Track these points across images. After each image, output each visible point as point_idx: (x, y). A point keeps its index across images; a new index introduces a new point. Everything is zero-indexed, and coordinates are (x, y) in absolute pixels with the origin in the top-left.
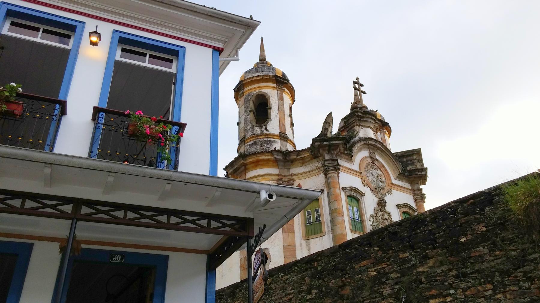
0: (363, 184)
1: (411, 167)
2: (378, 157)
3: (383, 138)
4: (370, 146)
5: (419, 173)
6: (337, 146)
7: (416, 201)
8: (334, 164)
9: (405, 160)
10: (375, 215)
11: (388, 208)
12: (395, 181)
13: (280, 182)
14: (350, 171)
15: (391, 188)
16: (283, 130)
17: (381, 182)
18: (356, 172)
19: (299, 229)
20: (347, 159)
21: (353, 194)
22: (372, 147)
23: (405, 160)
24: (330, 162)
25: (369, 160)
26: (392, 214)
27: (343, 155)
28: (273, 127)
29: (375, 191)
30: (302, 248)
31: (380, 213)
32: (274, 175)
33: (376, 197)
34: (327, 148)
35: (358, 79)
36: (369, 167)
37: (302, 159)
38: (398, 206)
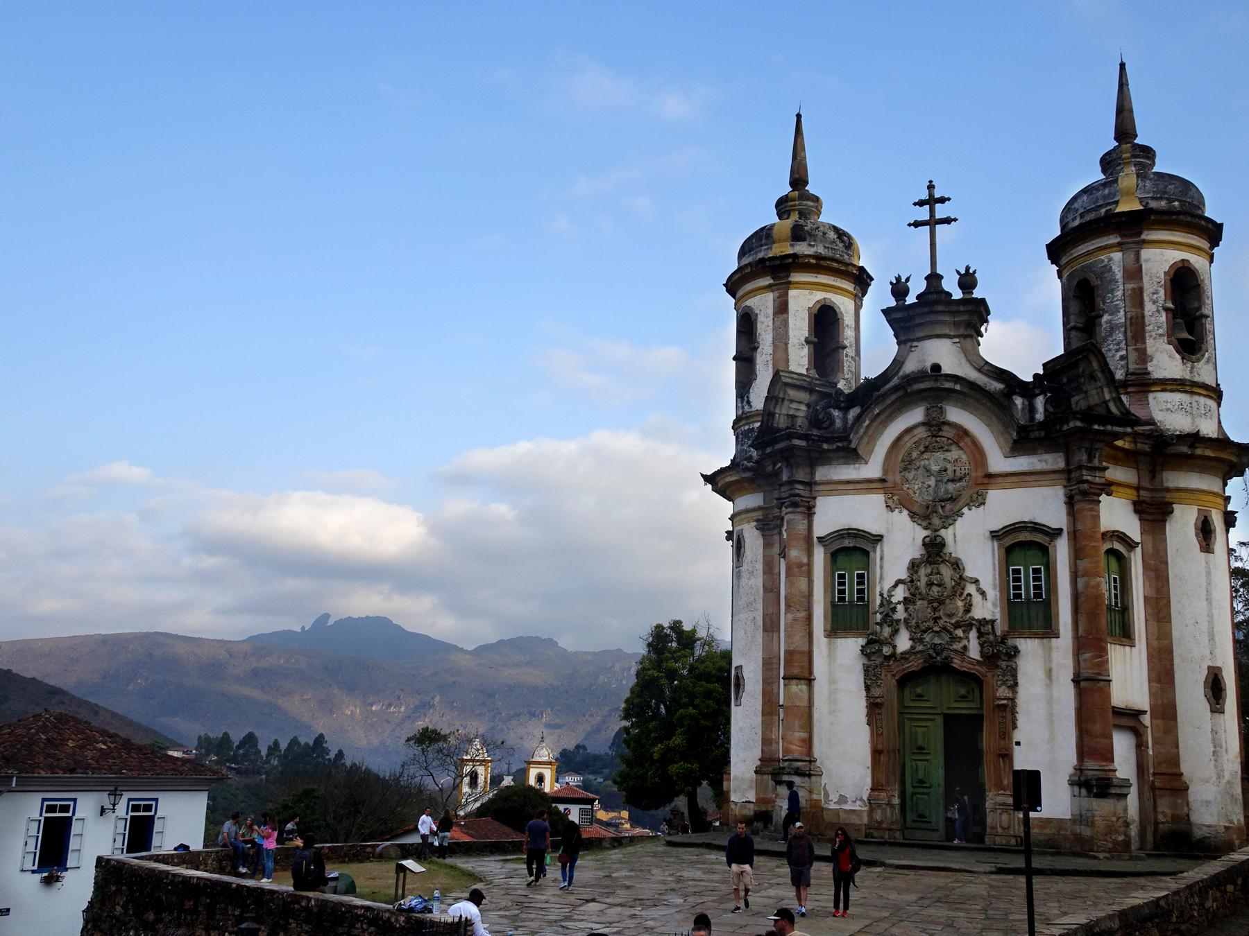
4: (924, 394)
5: (1065, 427)
7: (1070, 502)
14: (849, 487)
17: (952, 481)
18: (870, 481)
20: (845, 458)
21: (847, 543)
23: (1065, 380)
25: (921, 433)
27: (830, 455)
29: (922, 515)
32: (753, 510)
33: (926, 528)
35: (931, 187)
36: (915, 455)
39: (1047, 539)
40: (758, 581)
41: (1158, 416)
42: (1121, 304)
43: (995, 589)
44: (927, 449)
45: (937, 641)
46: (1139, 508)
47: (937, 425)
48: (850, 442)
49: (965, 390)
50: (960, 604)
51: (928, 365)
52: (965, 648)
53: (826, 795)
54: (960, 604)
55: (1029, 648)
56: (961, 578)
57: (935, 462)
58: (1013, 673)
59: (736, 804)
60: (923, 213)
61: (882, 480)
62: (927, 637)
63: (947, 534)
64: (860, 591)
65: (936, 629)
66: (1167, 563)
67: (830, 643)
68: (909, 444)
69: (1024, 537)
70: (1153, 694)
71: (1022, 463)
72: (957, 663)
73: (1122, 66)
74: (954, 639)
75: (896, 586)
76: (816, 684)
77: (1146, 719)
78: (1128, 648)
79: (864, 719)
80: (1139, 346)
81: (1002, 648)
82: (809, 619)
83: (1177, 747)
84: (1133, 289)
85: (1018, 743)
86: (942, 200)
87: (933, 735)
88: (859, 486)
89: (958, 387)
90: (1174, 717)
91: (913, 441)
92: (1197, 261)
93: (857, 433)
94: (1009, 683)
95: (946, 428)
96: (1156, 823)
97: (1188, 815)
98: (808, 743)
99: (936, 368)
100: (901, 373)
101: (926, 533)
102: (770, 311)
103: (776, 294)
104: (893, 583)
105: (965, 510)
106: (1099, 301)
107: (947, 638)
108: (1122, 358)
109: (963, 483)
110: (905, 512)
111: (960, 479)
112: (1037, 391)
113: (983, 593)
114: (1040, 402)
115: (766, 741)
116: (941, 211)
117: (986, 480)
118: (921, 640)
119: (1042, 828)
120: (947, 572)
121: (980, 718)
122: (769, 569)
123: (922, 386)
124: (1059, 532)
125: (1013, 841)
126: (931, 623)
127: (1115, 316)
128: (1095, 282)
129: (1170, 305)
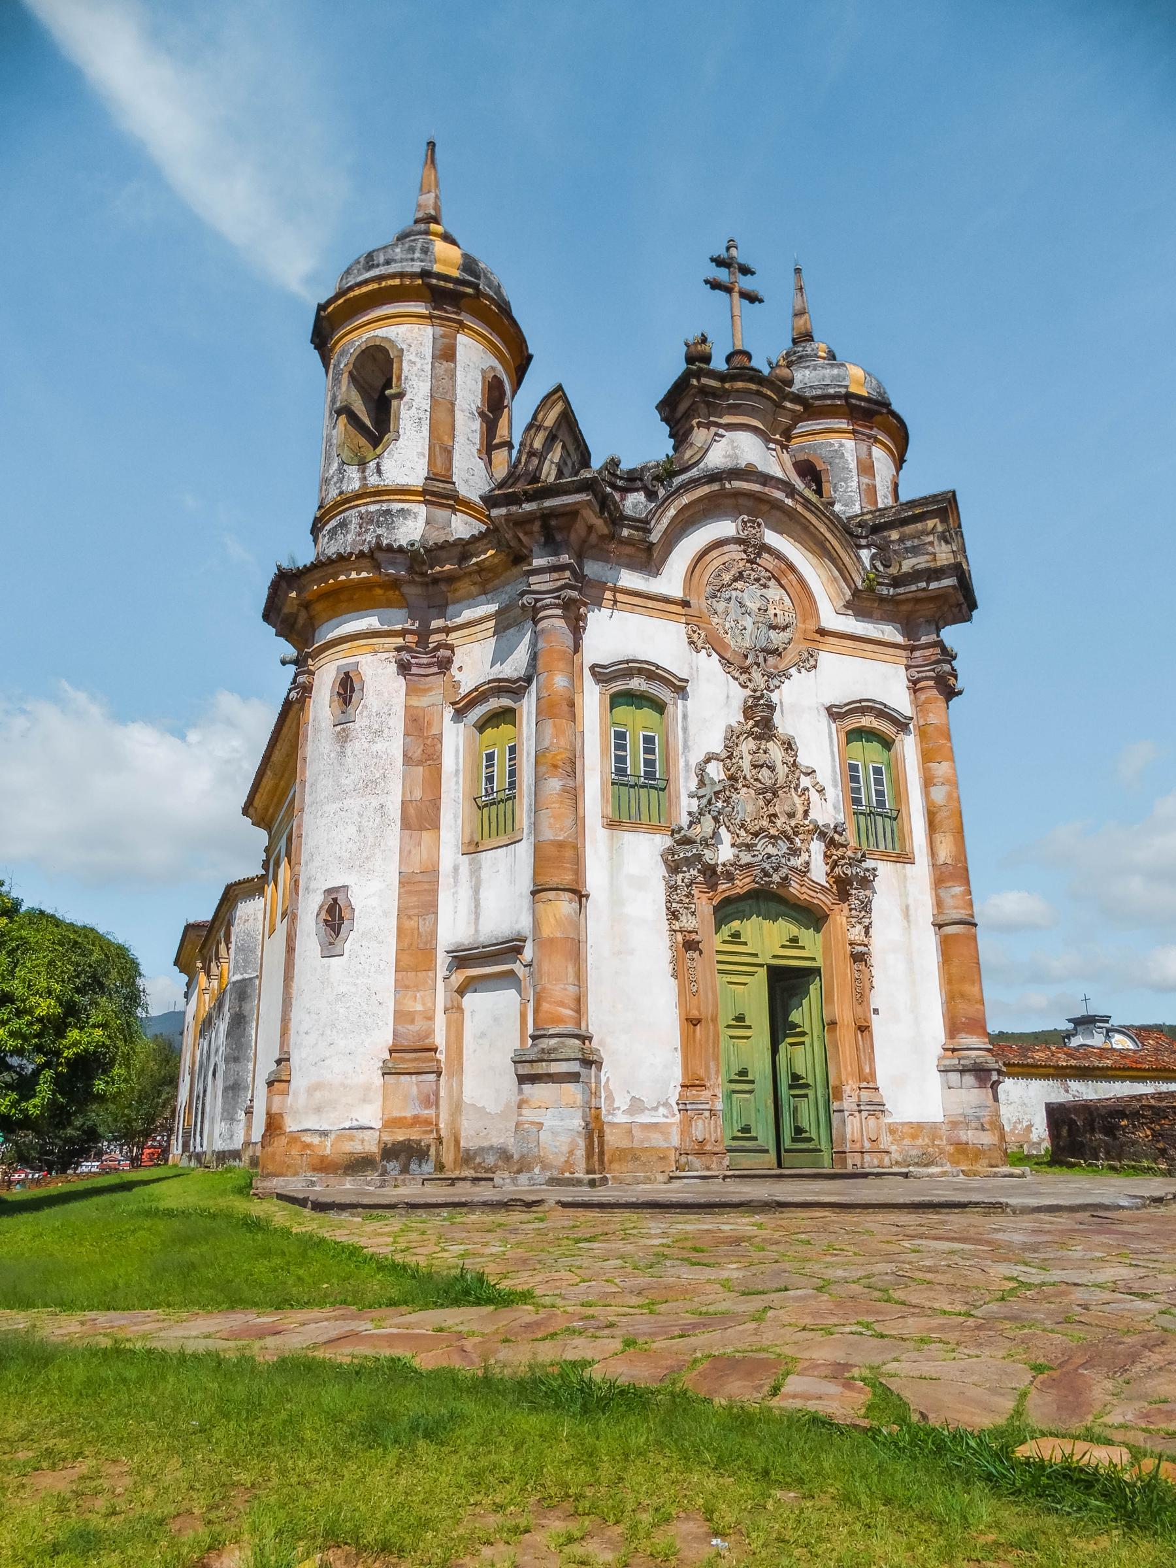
0: (692, 643)
1: (914, 561)
2: (772, 538)
3: (864, 456)
4: (741, 501)
6: (572, 514)
7: (915, 686)
8: (559, 583)
9: (894, 535)
10: (724, 755)
11: (783, 724)
12: (831, 617)
13: (405, 656)
15: (813, 645)
16: (440, 469)
18: (667, 600)
19: (455, 817)
21: (636, 684)
22: (750, 503)
24: (546, 577)
25: (734, 552)
26: (799, 743)
28: (405, 461)
29: (737, 665)
30: (456, 882)
31: (748, 745)
34: (536, 527)
37: (481, 568)
38: (835, 713)
40: (394, 746)
43: (836, 786)
44: (740, 577)
45: (771, 850)
48: (650, 531)
49: (800, 508)
53: (610, 1098)
54: (797, 800)
56: (794, 764)
57: (751, 596)
58: (866, 907)
59: (324, 1134)
60: (722, 275)
61: (685, 604)
62: (760, 844)
64: (649, 763)
65: (773, 832)
68: (716, 563)
72: (795, 888)
73: (798, 271)
74: (795, 852)
75: (708, 761)
79: (668, 968)
82: (574, 795)
84: (868, 485)
85: (876, 1011)
86: (746, 271)
87: (753, 996)
88: (650, 604)
89: (789, 502)
93: (658, 521)
95: (765, 555)
100: (702, 465)
102: (428, 351)
103: (440, 330)
104: (702, 757)
105: (793, 671)
107: (784, 846)
110: (715, 656)
111: (784, 628)
112: (863, 542)
113: (821, 791)
115: (401, 1016)
116: (745, 283)
117: (817, 637)
118: (749, 847)
120: (776, 753)
122: (419, 728)
128: (820, 466)
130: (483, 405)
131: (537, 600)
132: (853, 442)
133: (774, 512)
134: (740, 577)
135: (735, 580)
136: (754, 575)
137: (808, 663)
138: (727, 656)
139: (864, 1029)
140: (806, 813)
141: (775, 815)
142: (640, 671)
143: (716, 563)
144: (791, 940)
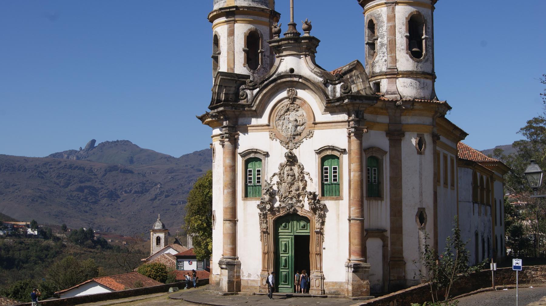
4: (287, 84)
25: (286, 102)
29: (285, 143)
39: (339, 153)
41: (401, 90)
42: (386, 34)
44: (288, 110)
45: (290, 202)
46: (389, 134)
47: (291, 99)
49: (304, 82)
50: (301, 185)
51: (288, 69)
52: (303, 206)
53: (243, 273)
55: (329, 204)
56: (302, 173)
61: (268, 125)
63: (295, 152)
66: (401, 161)
67: (244, 203)
69: (329, 153)
70: (392, 222)
71: (329, 117)
75: (273, 176)
76: (239, 224)
77: (388, 234)
78: (380, 202)
79: (259, 238)
80: (393, 55)
81: (318, 205)
83: (402, 246)
85: (324, 248)
88: (257, 128)
89: (300, 80)
90: (401, 232)
91: (282, 106)
92: (425, 11)
94: (321, 221)
96: (390, 280)
97: (404, 276)
98: (234, 250)
99: (292, 70)
101: (288, 151)
102: (226, 34)
106: (376, 31)
108: (386, 61)
109: (303, 127)
110: (278, 140)
111: (303, 125)
112: (337, 82)
114: (338, 87)
118: (283, 202)
119: (333, 286)
121: (308, 237)
123: (284, 80)
124: (344, 151)
125: (320, 293)
126: (288, 194)
127: (382, 40)
128: (375, 22)
129: (408, 34)
130: (245, 47)
131: (223, 137)
132: (386, 8)
133: (299, 84)
134: (288, 110)
135: (286, 112)
136: (293, 108)
137: (310, 135)
138: (282, 139)
139: (320, 254)
140: (304, 188)
141: (291, 191)
142: (253, 152)
143: (280, 108)
144: (302, 227)
